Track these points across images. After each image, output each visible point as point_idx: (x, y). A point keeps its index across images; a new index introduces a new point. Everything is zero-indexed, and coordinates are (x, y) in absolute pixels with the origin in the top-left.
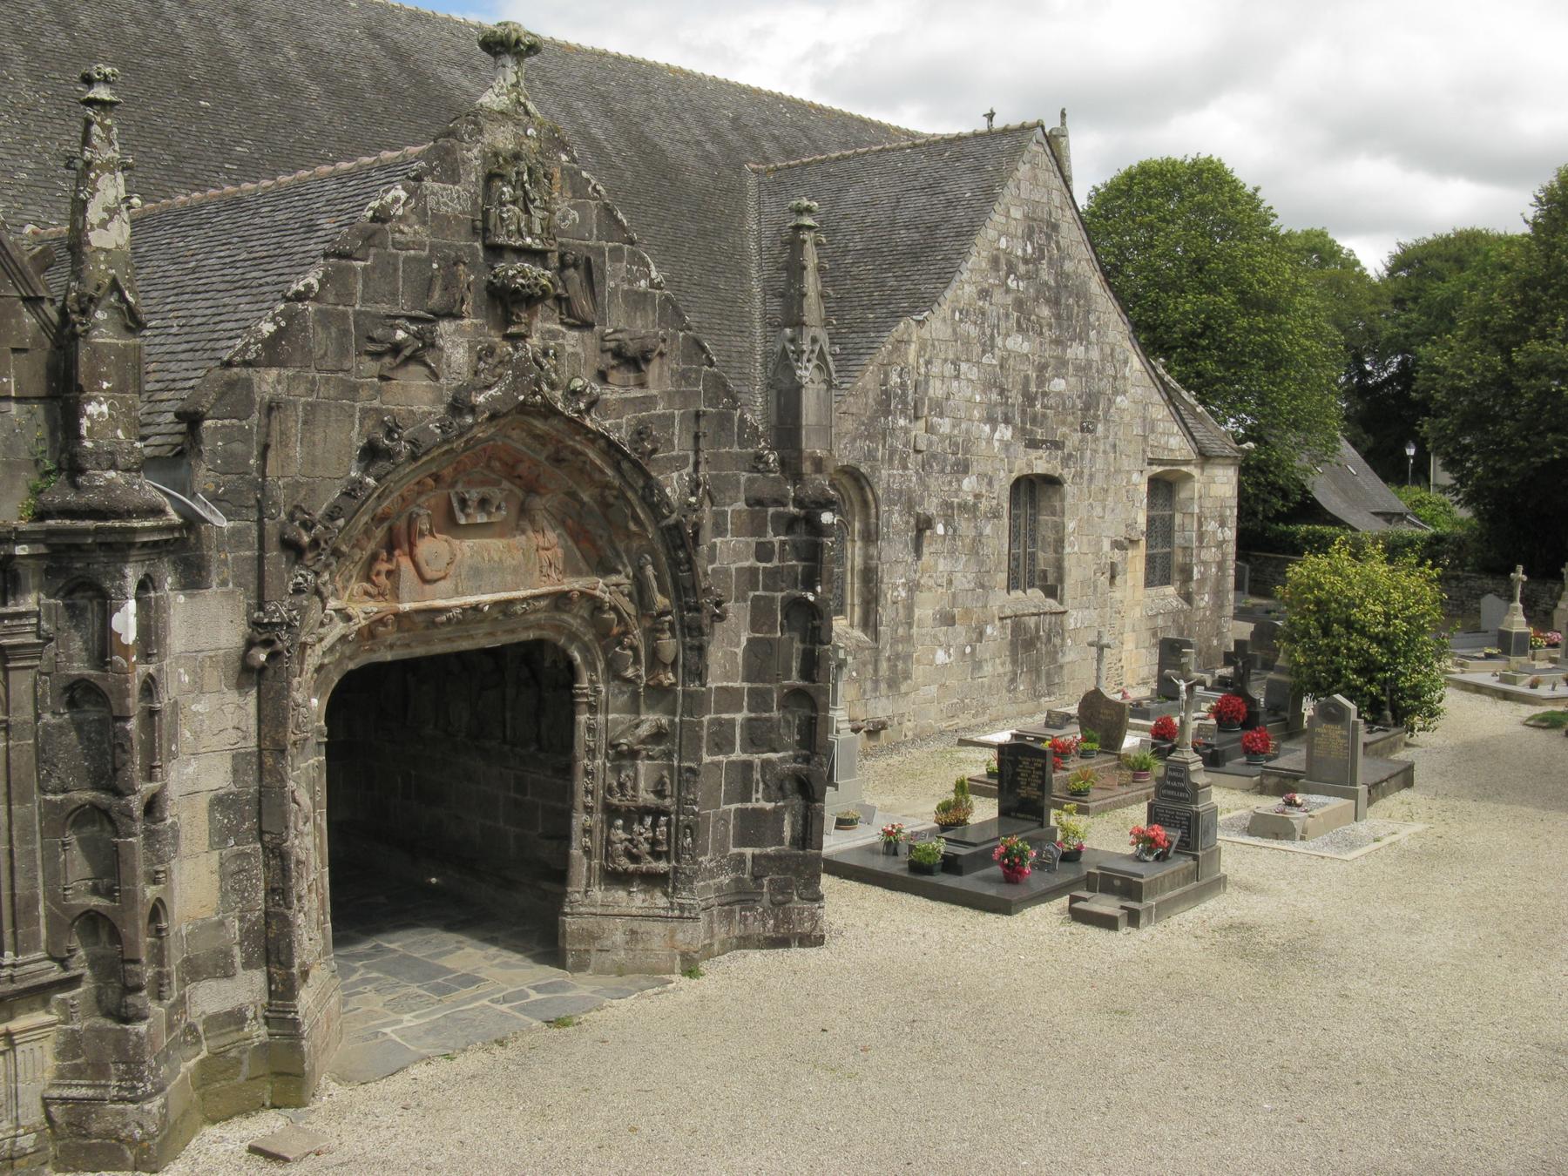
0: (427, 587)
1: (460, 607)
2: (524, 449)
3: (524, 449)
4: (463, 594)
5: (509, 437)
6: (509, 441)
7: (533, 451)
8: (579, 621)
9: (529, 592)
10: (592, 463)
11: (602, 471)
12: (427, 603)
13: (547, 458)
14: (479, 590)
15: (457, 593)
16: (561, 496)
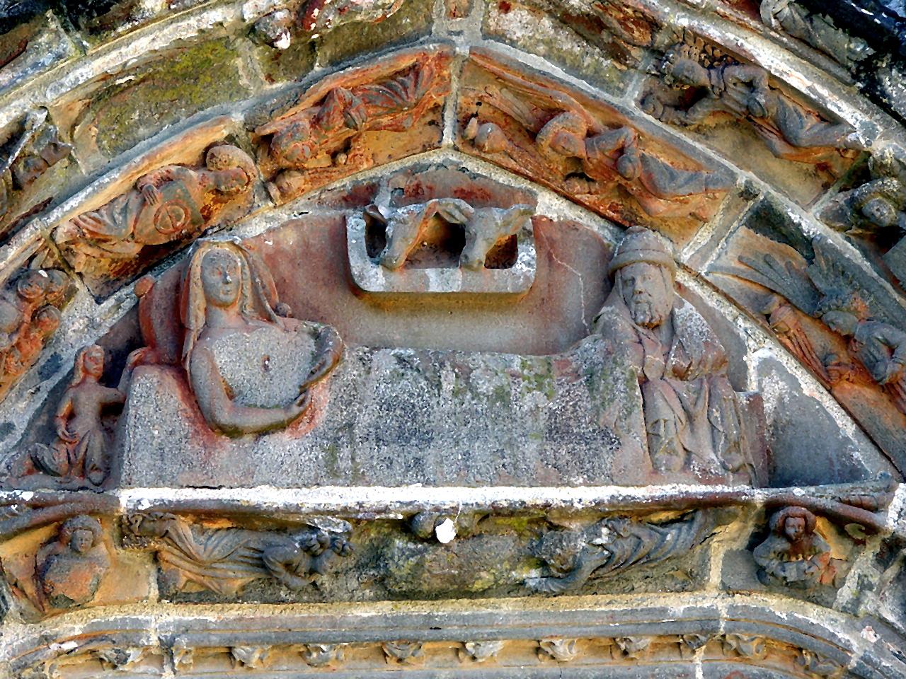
0: (227, 449)
1: (345, 513)
2: (559, 72)
3: (559, 72)
4: (357, 478)
5: (500, 37)
6: (501, 48)
7: (596, 79)
8: (870, 635)
9: (604, 493)
10: (778, 83)
11: (830, 119)
12: (225, 495)
13: (643, 102)
14: (417, 470)
15: (331, 473)
16: (743, 231)
